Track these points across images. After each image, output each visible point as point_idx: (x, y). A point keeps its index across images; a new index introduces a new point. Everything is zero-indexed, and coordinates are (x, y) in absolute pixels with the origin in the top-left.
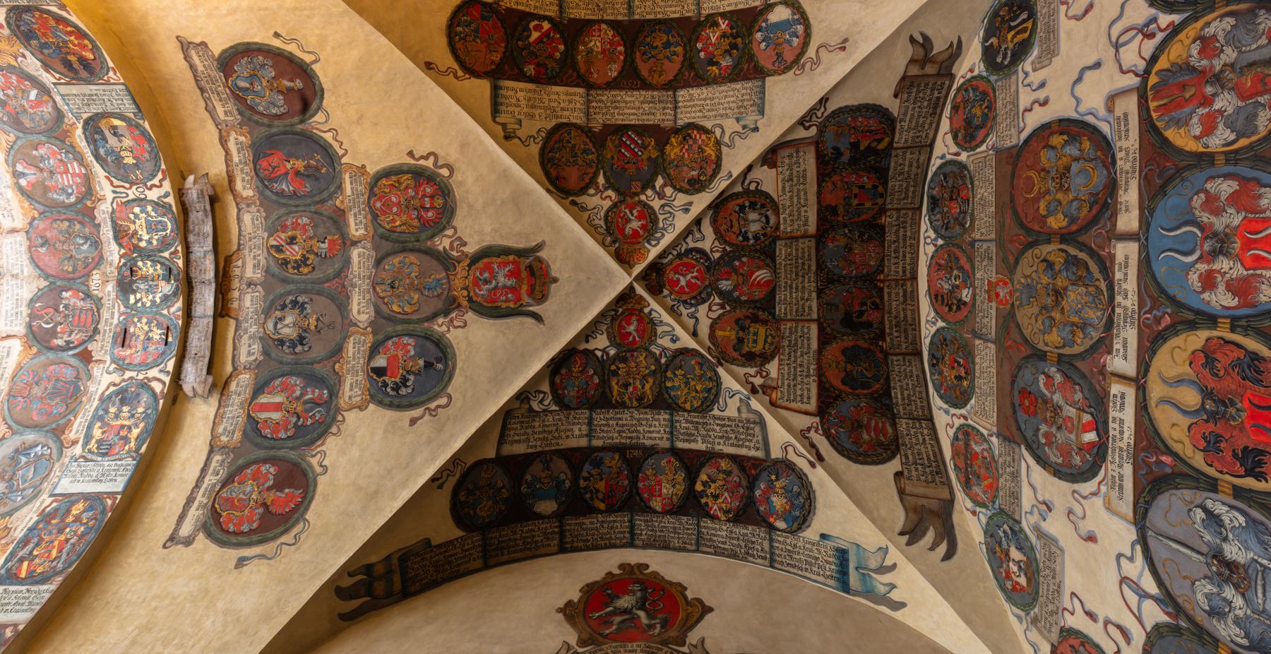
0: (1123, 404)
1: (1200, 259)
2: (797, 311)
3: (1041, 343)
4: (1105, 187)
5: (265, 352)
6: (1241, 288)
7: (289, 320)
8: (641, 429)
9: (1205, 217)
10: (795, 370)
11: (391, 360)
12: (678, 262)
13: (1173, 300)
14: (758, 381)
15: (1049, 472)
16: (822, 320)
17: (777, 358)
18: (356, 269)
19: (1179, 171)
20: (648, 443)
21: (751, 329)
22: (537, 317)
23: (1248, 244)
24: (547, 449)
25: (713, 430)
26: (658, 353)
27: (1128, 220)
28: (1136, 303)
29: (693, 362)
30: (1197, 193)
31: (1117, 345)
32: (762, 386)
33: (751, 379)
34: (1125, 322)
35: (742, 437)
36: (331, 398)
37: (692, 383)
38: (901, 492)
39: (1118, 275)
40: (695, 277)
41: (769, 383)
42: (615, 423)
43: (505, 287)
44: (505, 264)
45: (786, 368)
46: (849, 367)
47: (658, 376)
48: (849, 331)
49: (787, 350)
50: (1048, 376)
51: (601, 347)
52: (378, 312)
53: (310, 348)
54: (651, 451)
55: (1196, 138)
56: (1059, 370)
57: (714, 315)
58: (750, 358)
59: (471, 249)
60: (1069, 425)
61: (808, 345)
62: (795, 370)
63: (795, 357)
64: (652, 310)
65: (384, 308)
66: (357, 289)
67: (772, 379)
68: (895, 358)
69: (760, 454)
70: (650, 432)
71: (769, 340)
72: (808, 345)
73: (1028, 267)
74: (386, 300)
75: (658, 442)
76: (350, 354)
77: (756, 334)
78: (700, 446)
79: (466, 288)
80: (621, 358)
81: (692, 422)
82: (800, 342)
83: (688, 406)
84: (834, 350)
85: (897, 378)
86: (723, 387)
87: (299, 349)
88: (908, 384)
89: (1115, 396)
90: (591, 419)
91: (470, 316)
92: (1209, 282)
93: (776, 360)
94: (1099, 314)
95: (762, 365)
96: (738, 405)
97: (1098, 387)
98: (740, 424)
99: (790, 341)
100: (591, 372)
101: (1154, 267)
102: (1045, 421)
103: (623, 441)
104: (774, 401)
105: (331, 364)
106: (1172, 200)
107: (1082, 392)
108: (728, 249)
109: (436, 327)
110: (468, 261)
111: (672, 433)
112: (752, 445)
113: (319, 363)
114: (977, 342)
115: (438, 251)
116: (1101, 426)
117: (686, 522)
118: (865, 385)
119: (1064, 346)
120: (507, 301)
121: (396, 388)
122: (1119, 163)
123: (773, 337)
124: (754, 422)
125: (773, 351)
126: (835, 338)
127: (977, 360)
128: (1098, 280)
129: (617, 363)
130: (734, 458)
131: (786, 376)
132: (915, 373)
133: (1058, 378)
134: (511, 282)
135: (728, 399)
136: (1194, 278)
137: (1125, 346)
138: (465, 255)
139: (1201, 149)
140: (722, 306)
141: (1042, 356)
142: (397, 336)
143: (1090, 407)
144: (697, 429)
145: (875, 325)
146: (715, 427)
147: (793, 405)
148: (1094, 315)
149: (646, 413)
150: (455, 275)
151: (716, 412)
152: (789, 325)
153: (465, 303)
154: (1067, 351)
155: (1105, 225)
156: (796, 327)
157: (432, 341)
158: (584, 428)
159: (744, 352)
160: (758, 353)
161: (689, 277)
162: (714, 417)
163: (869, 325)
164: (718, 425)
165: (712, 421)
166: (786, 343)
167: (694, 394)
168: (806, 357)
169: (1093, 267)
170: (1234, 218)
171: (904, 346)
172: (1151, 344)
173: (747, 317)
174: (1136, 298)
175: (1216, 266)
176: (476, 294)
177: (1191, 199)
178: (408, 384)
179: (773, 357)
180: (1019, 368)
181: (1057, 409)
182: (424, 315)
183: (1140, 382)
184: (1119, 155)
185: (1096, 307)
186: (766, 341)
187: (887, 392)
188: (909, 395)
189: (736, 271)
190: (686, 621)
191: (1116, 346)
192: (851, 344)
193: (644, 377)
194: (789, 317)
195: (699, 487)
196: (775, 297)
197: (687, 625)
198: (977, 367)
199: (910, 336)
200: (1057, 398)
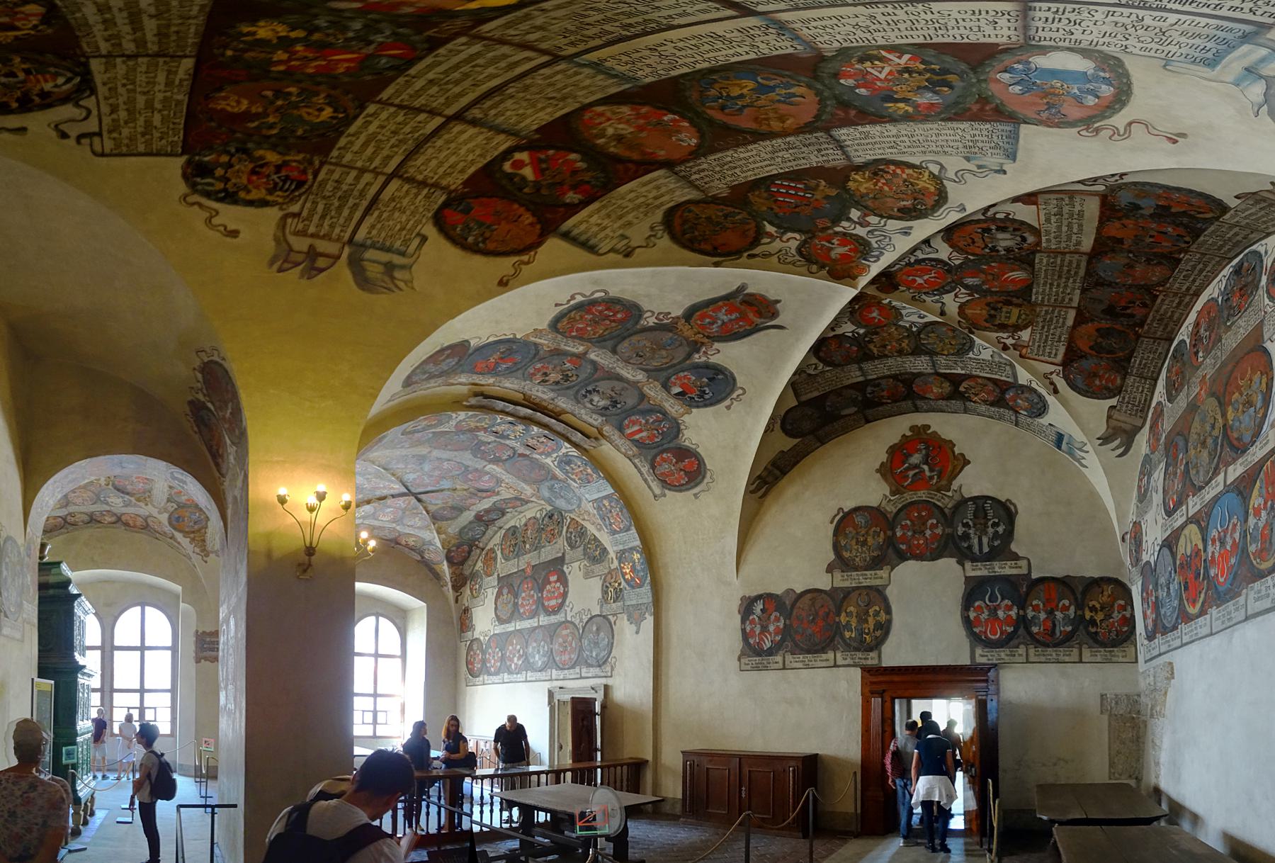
118: (1109, 352)
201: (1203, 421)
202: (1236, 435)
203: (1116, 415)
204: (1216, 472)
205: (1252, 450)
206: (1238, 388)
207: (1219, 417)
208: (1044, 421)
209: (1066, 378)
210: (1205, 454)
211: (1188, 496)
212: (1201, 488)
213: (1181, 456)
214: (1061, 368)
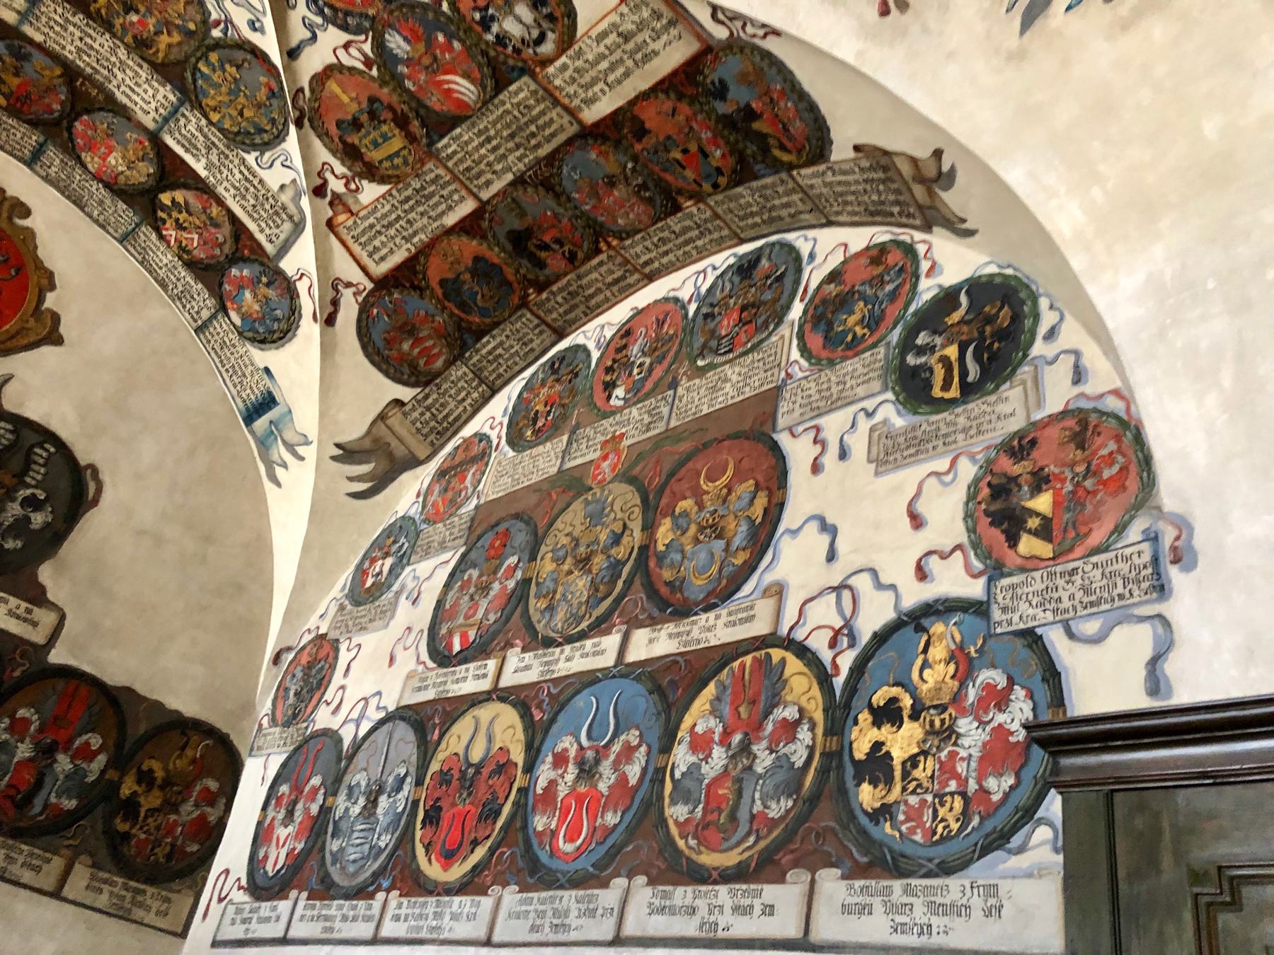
1: (581, 748)
2: (468, 169)
10: (399, 218)
14: (336, 185)
16: (489, 208)
17: (387, 187)
21: (385, 128)
23: (580, 800)
26: (214, 16)
32: (336, 196)
33: (328, 175)
34: (547, 663)
37: (242, 100)
41: (350, 201)
42: (78, 34)
45: (388, 207)
46: (467, 276)
47: (194, 43)
48: (509, 247)
49: (409, 192)
57: (346, 61)
58: (350, 153)
61: (443, 213)
62: (399, 218)
63: (412, 209)
67: (357, 201)
68: (529, 315)
69: (270, 249)
71: (396, 161)
72: (443, 213)
75: (137, 109)
77: (386, 138)
78: (199, 167)
81: (205, 136)
82: (436, 199)
84: (469, 247)
85: (508, 332)
86: (283, 145)
88: (512, 347)
93: (384, 188)
94: (560, 625)
95: (361, 176)
96: (287, 181)
99: (423, 188)
104: (335, 222)
112: (267, 231)
117: (124, 215)
118: (463, 306)
123: (406, 163)
124: (291, 217)
125: (390, 177)
126: (484, 237)
130: (234, 219)
131: (379, 215)
132: (534, 345)
135: (277, 163)
140: (368, 63)
144: (209, 149)
145: (547, 271)
146: (236, 171)
147: (356, 249)
151: (250, 158)
152: (441, 171)
156: (448, 183)
159: (349, 140)
160: (366, 159)
162: (243, 161)
163: (541, 265)
164: (241, 172)
165: (236, 162)
166: (416, 184)
168: (425, 220)
171: (554, 315)
173: (391, 108)
179: (382, 180)
186: (390, 158)
187: (479, 334)
188: (500, 355)
189: (430, 43)
190: (13, 337)
192: (496, 260)
193: (168, 23)
194: (450, 164)
196: (453, 128)
197: (9, 344)
199: (572, 315)
201: (595, 518)
202: (667, 575)
203: (395, 420)
204: (600, 626)
205: (704, 619)
206: (698, 494)
207: (636, 526)
209: (364, 309)
210: (581, 584)
211: (509, 645)
212: (549, 643)
213: (512, 560)
214: (370, 286)
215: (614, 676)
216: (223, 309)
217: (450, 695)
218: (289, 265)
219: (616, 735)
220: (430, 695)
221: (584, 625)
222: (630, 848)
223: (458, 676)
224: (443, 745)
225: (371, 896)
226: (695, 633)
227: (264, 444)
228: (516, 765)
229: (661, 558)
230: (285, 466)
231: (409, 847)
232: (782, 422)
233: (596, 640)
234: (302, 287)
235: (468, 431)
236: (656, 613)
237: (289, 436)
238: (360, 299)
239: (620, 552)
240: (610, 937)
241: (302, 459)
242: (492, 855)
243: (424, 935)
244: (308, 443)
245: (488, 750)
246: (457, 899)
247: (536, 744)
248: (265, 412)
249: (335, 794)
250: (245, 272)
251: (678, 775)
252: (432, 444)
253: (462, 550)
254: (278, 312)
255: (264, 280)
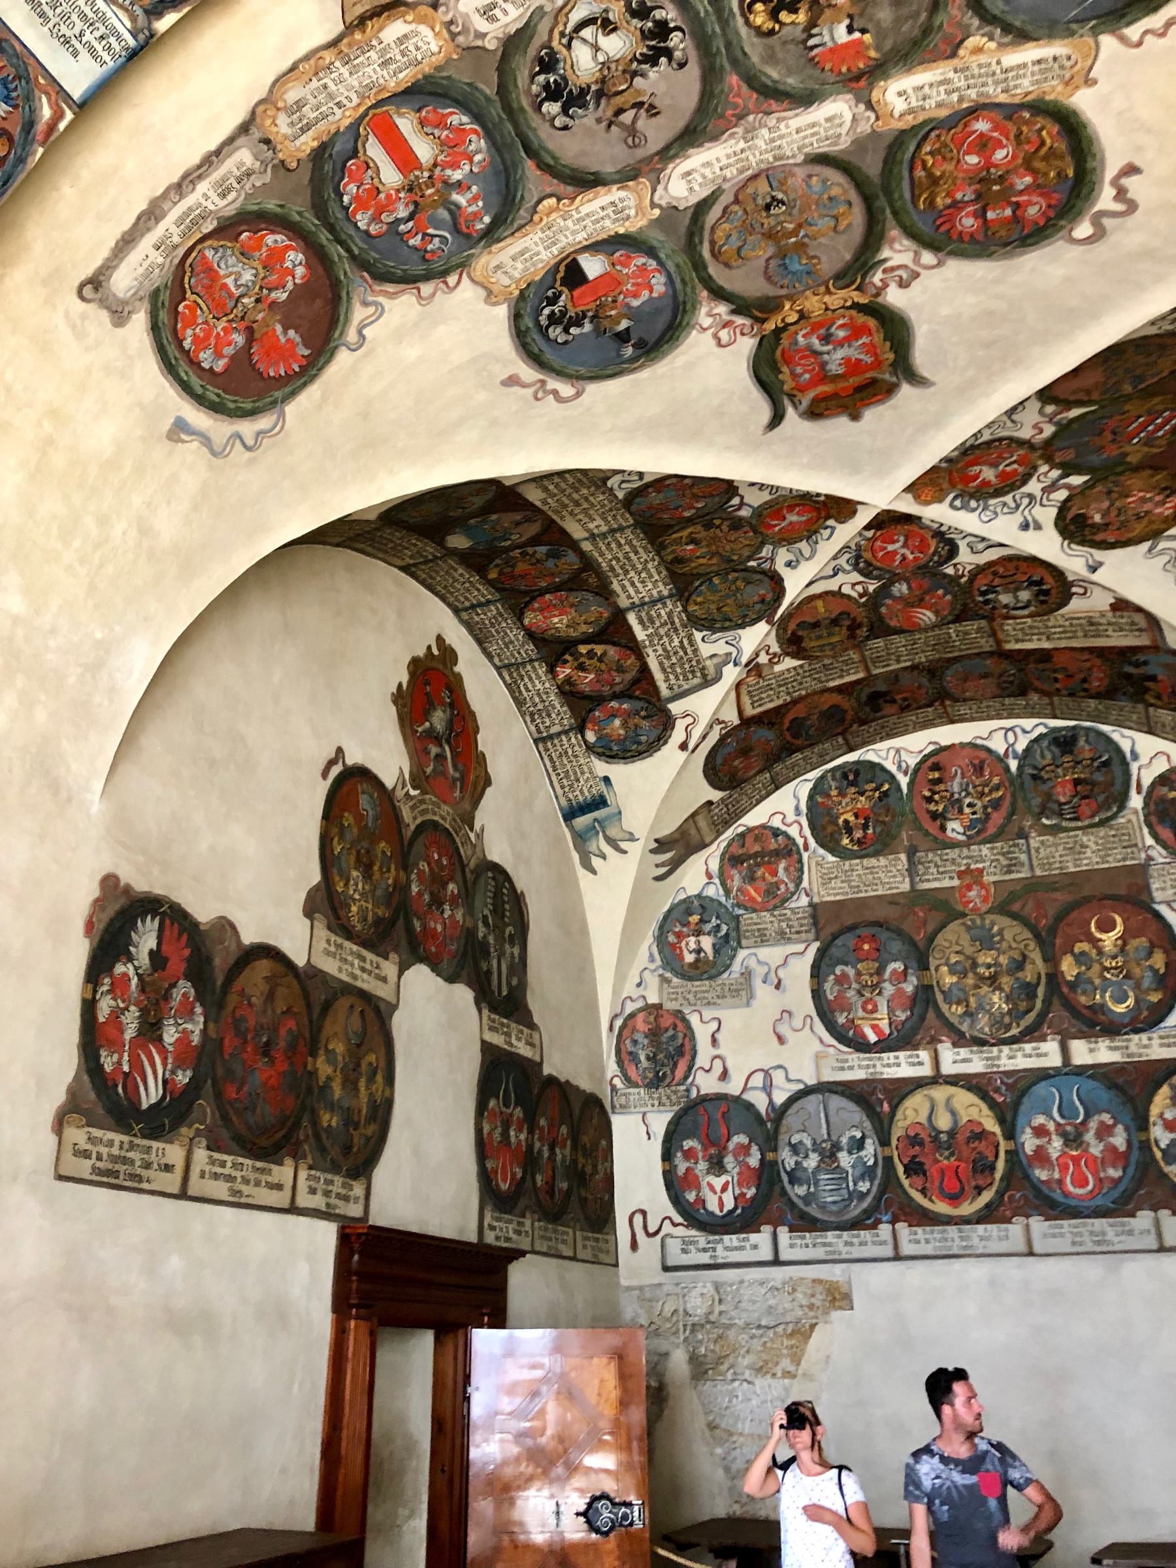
0: (913, 1064)
1: (1058, 1125)
3: (938, 962)
4: (1112, 1022)
5: (514, 42)
6: (1041, 1156)
7: (616, 45)
8: (632, 574)
9: (1093, 1124)
11: (609, 280)
12: (929, 535)
13: (1017, 1104)
15: (812, 985)
18: (795, 123)
19: (1130, 1100)
20: (616, 586)
22: (777, 419)
23: (1076, 1160)
24: (550, 513)
25: (671, 641)
27: (1083, 1053)
28: (1007, 1068)
29: (762, 592)
30: (1113, 1117)
31: (964, 1052)
34: (988, 1059)
35: (679, 670)
36: (481, 238)
38: (693, 815)
39: (1028, 1047)
40: (904, 557)
43: (823, 365)
44: (871, 349)
50: (905, 973)
51: (745, 501)
52: (702, 207)
53: (565, 128)
54: (604, 592)
55: (1161, 1116)
56: (916, 987)
59: (894, 297)
60: (870, 1007)
64: (833, 529)
65: (715, 212)
66: (742, 144)
69: (664, 692)
70: (633, 584)
73: (1012, 932)
74: (736, 208)
75: (623, 596)
76: (585, 209)
78: (640, 634)
79: (803, 315)
80: (737, 524)
83: (691, 608)
86: (740, 631)
87: (551, 108)
89: (918, 1056)
90: (621, 529)
91: (747, 345)
92: (1040, 1131)
94: (987, 1029)
97: (919, 1037)
98: (694, 663)
100: (699, 505)
101: (1043, 1083)
102: (859, 974)
103: (604, 565)
105: (548, 190)
106: (1103, 1095)
107: (907, 1020)
108: (964, 580)
109: (704, 310)
110: (863, 300)
111: (643, 604)
113: (543, 167)
114: (903, 856)
115: (878, 249)
116: (885, 1045)
119: (943, 992)
120: (794, 375)
121: (553, 320)
122: (1135, 1037)
127: (883, 861)
128: (1018, 1025)
129: (726, 523)
130: (645, 670)
133: (909, 988)
134: (835, 368)
136: (1040, 1120)
137: (964, 1061)
138: (879, 291)
139: (1152, 1119)
141: (924, 966)
142: (660, 263)
143: (898, 1031)
148: (983, 1024)
149: (659, 573)
150: (828, 292)
151: (698, 636)
153: (770, 326)
154: (939, 997)
155: (1074, 1026)
157: (675, 317)
158: (604, 529)
161: (904, 551)
164: (681, 642)
167: (713, 607)
169: (1031, 1018)
170: (1096, 1149)
172: (974, 1084)
174: (1012, 1068)
175: (1054, 1137)
176: (796, 333)
177: (1108, 1112)
178: (573, 330)
180: (899, 932)
181: (876, 987)
182: (721, 282)
183: (937, 1079)
184: (1144, 1037)
185: (992, 1026)
191: (962, 1050)
195: (583, 649)
198: (873, 862)
200: (889, 989)
204: (1032, 1033)
208: (601, 768)
215: (1066, 1074)
216: (581, 730)
217: (885, 1076)
218: (675, 708)
219: (1088, 1116)
220: (859, 1075)
221: (1015, 1031)
222: (1142, 1192)
223: (886, 1062)
224: (899, 1115)
225: (874, 1226)
226: (1133, 1048)
227: (581, 839)
228: (994, 1134)
229: (1073, 986)
230: (604, 857)
231: (899, 1191)
232: (1158, 895)
233: (1034, 1045)
234: (680, 725)
235: (754, 818)
236: (1085, 1029)
237: (612, 832)
238: (724, 732)
239: (1028, 975)
240: (1154, 1245)
241: (625, 852)
242: (1003, 1195)
243: (955, 1251)
244: (632, 838)
245: (956, 1122)
246: (980, 1228)
247: (1009, 1117)
248: (590, 812)
249: (775, 1150)
250: (625, 706)
251: (1163, 1146)
252: (718, 831)
253: (816, 945)
254: (643, 739)
255: (643, 713)
